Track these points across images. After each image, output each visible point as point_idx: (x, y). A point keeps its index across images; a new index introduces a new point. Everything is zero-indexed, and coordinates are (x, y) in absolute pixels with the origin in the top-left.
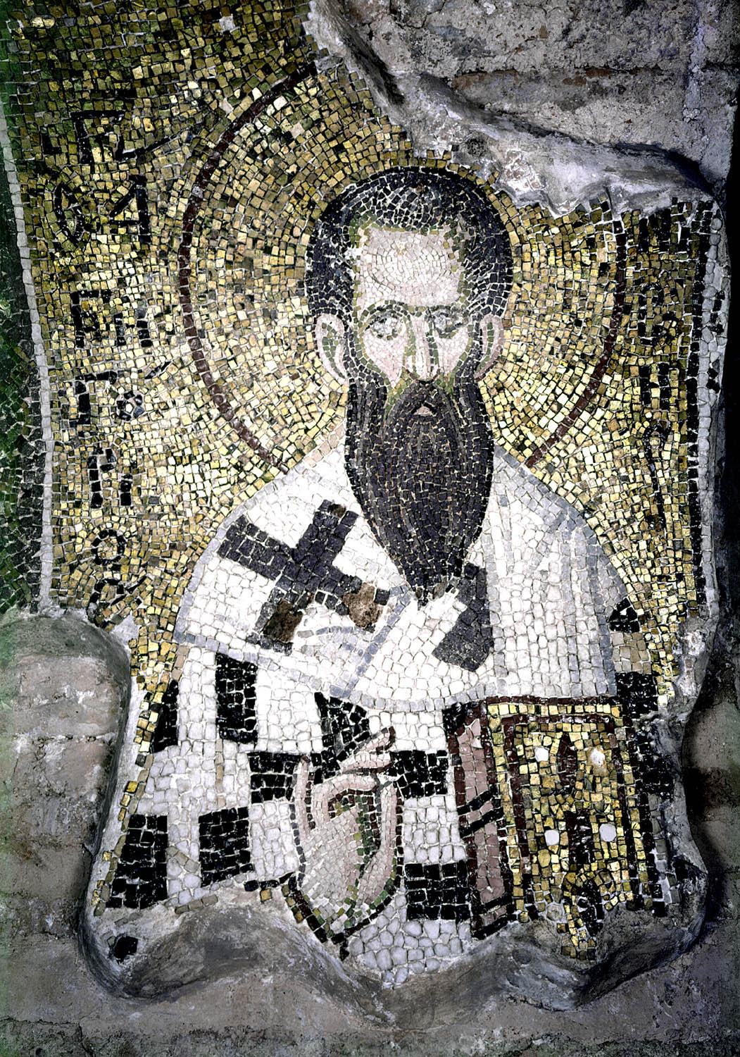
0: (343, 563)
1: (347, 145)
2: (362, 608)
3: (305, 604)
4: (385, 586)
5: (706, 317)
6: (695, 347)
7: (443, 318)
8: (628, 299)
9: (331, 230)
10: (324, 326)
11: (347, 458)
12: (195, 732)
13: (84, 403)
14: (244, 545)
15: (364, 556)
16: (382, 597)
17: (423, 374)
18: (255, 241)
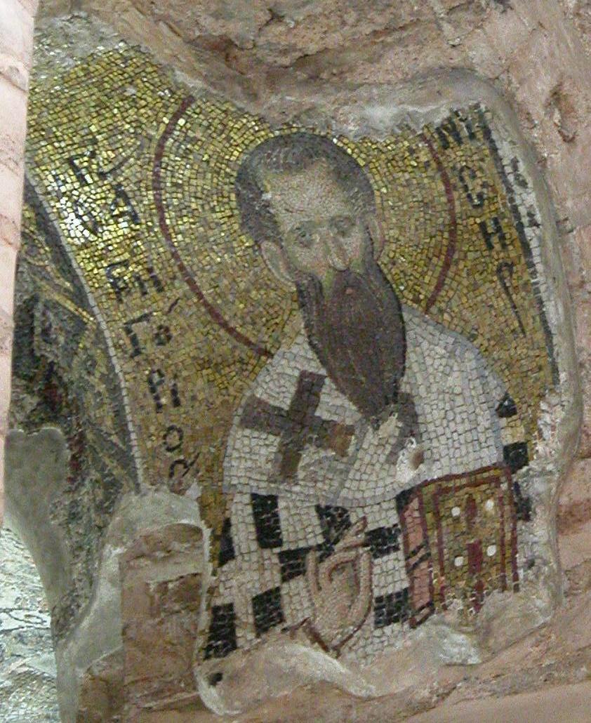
0: (322, 413)
1: (232, 134)
2: (338, 440)
3: (301, 448)
4: (349, 422)
5: (511, 178)
6: (512, 200)
7: (341, 226)
8: (452, 181)
9: (248, 186)
10: (267, 250)
11: (309, 337)
12: (244, 549)
13: (134, 340)
14: (260, 417)
15: (334, 404)
16: (350, 430)
17: (340, 265)
18: (203, 206)
